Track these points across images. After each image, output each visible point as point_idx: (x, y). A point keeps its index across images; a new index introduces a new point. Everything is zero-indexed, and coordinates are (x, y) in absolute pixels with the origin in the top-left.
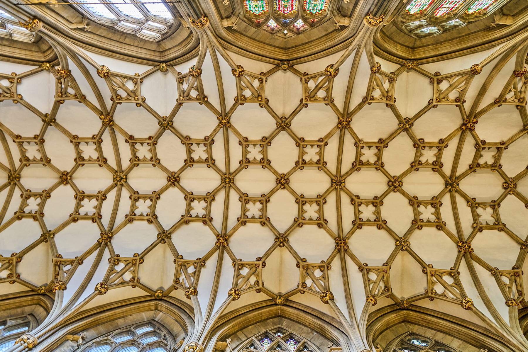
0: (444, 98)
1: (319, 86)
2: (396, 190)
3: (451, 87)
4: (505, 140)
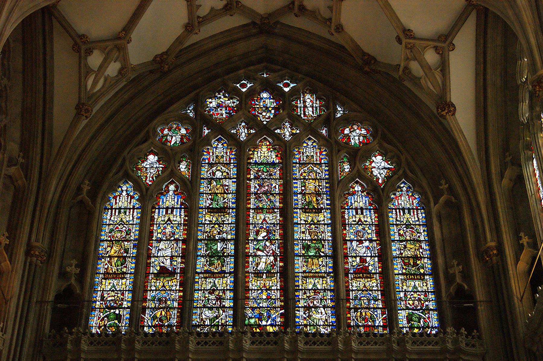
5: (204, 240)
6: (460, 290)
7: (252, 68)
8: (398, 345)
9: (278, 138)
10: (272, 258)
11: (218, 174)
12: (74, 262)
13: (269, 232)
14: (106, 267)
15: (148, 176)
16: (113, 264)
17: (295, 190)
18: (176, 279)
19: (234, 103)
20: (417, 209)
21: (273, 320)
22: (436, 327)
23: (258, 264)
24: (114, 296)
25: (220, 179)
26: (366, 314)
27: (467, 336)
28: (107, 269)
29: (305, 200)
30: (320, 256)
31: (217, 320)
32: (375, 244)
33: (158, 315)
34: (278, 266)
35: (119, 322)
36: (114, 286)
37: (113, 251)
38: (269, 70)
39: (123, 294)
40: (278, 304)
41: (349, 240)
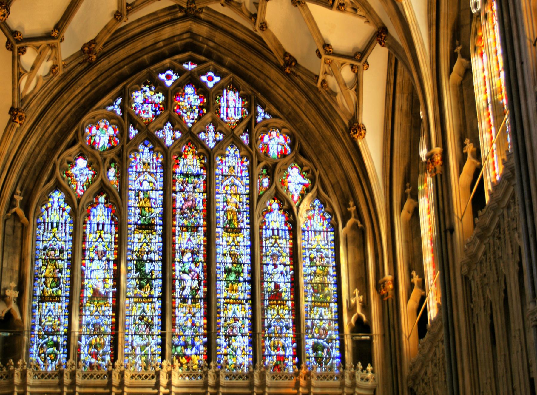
5: (134, 260)
7: (177, 57)
9: (201, 144)
10: (196, 282)
11: (146, 186)
13: (193, 253)
14: (42, 288)
15: (79, 184)
16: (49, 285)
17: (218, 205)
18: (109, 303)
20: (327, 232)
21: (197, 348)
22: (337, 358)
23: (183, 289)
24: (51, 321)
25: (147, 191)
26: (278, 343)
28: (43, 291)
29: (227, 217)
31: (147, 348)
32: (288, 268)
33: (94, 342)
34: (202, 291)
35: (58, 349)
36: (50, 310)
37: (48, 270)
38: (194, 61)
39: (59, 319)
40: (202, 331)
41: (265, 264)
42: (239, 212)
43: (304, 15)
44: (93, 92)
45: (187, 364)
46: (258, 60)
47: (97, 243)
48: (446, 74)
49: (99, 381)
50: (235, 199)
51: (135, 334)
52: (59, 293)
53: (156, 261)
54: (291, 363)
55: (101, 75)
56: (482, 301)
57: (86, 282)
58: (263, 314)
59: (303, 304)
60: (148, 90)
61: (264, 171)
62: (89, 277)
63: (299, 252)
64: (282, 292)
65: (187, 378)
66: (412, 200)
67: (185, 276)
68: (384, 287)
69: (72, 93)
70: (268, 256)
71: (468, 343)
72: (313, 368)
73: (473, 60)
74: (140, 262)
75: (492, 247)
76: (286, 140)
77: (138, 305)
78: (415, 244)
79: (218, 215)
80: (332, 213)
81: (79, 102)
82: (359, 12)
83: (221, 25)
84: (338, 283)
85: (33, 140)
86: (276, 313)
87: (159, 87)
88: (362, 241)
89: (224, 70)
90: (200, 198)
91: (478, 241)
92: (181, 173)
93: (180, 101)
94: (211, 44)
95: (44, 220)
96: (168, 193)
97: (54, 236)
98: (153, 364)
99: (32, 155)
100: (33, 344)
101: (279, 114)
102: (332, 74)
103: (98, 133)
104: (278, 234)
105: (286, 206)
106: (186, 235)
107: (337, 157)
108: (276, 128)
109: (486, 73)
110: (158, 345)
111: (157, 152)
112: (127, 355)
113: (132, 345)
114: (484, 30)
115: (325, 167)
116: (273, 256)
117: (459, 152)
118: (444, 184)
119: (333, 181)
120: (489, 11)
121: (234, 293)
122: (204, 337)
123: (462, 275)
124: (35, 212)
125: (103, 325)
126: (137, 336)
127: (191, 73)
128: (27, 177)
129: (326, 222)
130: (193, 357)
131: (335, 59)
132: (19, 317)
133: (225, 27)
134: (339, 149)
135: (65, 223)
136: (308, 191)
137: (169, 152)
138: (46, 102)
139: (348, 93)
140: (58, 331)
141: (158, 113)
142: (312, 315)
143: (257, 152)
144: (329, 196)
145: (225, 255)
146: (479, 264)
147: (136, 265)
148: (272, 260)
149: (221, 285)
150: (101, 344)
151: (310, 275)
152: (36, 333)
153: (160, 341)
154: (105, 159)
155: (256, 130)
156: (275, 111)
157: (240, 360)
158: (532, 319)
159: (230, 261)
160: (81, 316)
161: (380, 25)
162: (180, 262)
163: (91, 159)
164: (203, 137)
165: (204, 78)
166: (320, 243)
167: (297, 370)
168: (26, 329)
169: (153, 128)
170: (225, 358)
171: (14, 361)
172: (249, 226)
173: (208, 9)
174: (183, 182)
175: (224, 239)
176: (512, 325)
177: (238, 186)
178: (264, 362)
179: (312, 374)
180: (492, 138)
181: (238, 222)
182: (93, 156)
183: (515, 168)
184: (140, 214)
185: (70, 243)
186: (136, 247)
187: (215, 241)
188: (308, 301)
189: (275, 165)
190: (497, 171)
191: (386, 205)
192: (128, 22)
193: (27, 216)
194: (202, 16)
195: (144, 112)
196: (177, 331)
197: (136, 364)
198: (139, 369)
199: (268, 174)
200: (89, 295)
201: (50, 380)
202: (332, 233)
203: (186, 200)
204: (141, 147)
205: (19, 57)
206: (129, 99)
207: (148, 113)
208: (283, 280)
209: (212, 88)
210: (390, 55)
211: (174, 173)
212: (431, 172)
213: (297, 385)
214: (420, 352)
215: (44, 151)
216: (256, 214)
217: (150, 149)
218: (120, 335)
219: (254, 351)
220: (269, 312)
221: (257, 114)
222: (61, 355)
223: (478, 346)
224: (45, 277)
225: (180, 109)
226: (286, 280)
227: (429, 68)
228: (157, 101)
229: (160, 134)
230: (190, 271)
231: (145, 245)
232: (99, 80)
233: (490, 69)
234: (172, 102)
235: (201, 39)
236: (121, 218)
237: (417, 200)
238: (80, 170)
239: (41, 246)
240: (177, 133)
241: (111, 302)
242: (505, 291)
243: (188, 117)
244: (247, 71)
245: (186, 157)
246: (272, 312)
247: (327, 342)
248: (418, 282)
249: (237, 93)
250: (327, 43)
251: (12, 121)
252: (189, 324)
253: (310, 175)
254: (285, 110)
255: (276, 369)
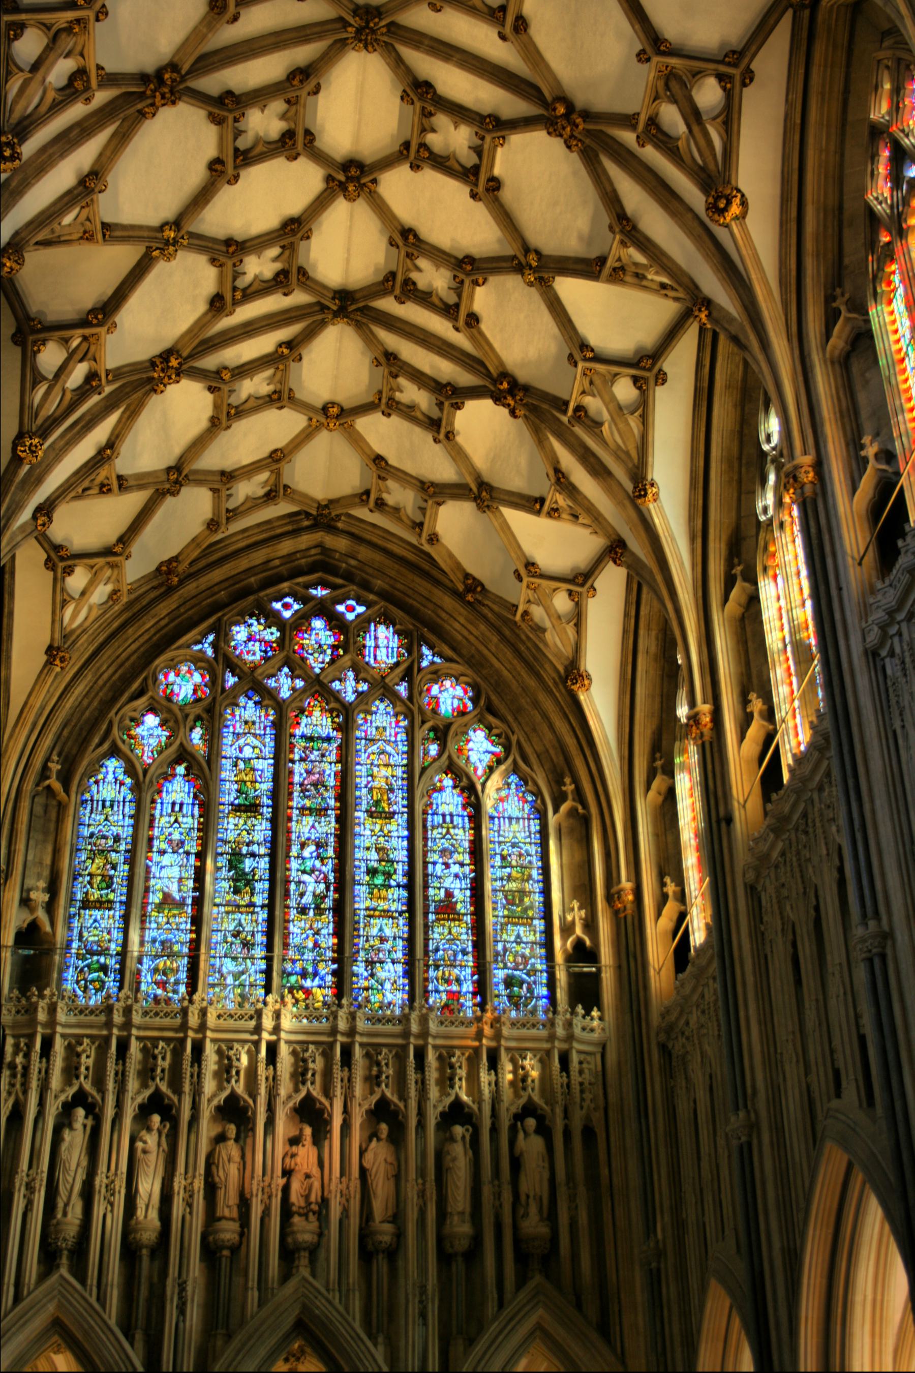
0: (591, 383)
1: (696, 129)
2: (331, 184)
3: (619, 409)
4: (459, 439)
6: (579, 944)
7: (300, 580)
8: (492, 1026)
9: (335, 696)
10: (322, 886)
11: (248, 752)
12: (42, 884)
13: (318, 845)
15: (146, 749)
16: (95, 886)
17: (358, 780)
19: (272, 634)
20: (529, 819)
21: (322, 979)
22: (543, 997)
23: (302, 895)
25: (250, 759)
27: (584, 1017)
30: (390, 886)
31: (243, 977)
32: (467, 869)
33: (161, 966)
35: (106, 975)
36: (95, 921)
37: (95, 866)
38: (325, 585)
39: (109, 933)
40: (330, 954)
42: (392, 790)
43: (496, 524)
44: (172, 625)
45: (304, 1000)
46: (424, 583)
47: (171, 830)
48: (719, 603)
49: (167, 1021)
50: (386, 772)
51: (226, 956)
52: (111, 896)
53: (260, 856)
54: (469, 1004)
55: (184, 603)
56: (779, 922)
57: (152, 882)
58: (426, 933)
59: (490, 919)
60: (255, 623)
61: (432, 735)
62: (157, 875)
63: (484, 846)
64: (456, 903)
65: (305, 1021)
66: (665, 777)
67: (305, 878)
68: (619, 898)
69: (140, 627)
70: (435, 852)
71: (756, 982)
72: (504, 1011)
73: (761, 584)
74: (236, 858)
75: (794, 844)
76: (466, 692)
77: (231, 916)
78: (670, 838)
79: (358, 793)
80: (538, 794)
81: (150, 639)
82: (581, 520)
83: (368, 536)
84: (546, 892)
85: (80, 689)
86: (446, 931)
87: (271, 619)
88: (584, 832)
89: (372, 597)
90: (330, 770)
91: (772, 836)
92: (303, 736)
93: (303, 638)
94: (353, 562)
95: (92, 797)
96: (282, 762)
97: (106, 819)
98: (252, 999)
99: (78, 708)
100: (68, 967)
101: (455, 657)
102: (539, 603)
103: (178, 680)
104: (452, 822)
105: (465, 782)
106: (310, 820)
107: (545, 717)
108: (451, 676)
109: (782, 602)
110: (261, 972)
111: (267, 707)
112: (213, 986)
113: (220, 971)
114: (778, 543)
115: (526, 729)
116: (443, 852)
117: (740, 712)
118: (716, 755)
119: (539, 748)
120: (786, 518)
121: (381, 903)
122: (333, 963)
123: (745, 884)
124: (79, 785)
125: (177, 942)
126: (229, 960)
127: (322, 600)
128: (68, 738)
129: (527, 807)
130: (314, 990)
131: (544, 583)
132: (48, 929)
133: (375, 540)
134: (549, 705)
135: (124, 802)
136: (499, 762)
137: (284, 707)
138: (101, 639)
139: (564, 629)
140: (108, 949)
141: (270, 654)
142: (505, 936)
143: (420, 708)
144: (532, 769)
145: (368, 849)
146: (773, 869)
147: (230, 861)
148: (441, 857)
149: (361, 891)
150: (172, 970)
151: (502, 879)
152: (73, 951)
153: (264, 967)
154: (186, 716)
155: (419, 678)
156: (449, 652)
157: (389, 997)
158: (861, 950)
159: (376, 857)
160: (143, 929)
161: (614, 537)
162: (298, 857)
163: (165, 715)
164: (338, 687)
165: (341, 608)
166: (518, 835)
167: (479, 1013)
168: (59, 946)
169: (261, 674)
170: (365, 994)
171: (38, 989)
172: (406, 810)
173: (349, 516)
174: (306, 748)
175: (367, 826)
176: (829, 957)
177: (390, 755)
178: (427, 1001)
179: (503, 1019)
180: (792, 692)
181: (389, 804)
182: (170, 711)
183: (831, 734)
184: (238, 791)
185: (131, 829)
186: (231, 836)
187: (353, 829)
188: (497, 916)
189: (448, 726)
190: (801, 738)
191: (623, 783)
192: (227, 533)
193: (67, 791)
194: (340, 525)
195: (248, 652)
196: (291, 953)
197: (225, 998)
198: (231, 1006)
199: (437, 738)
200: (157, 901)
201: (93, 1017)
202: (537, 822)
203: (309, 772)
204: (242, 700)
205: (63, 579)
206: (226, 635)
207: (254, 654)
208: (458, 886)
209: (353, 621)
210: (629, 579)
211: (293, 735)
212: (695, 739)
213: (479, 1035)
214: (678, 993)
215: (95, 703)
216: (418, 794)
217: (256, 703)
218: (203, 957)
219: (412, 984)
220: (436, 930)
221: (421, 656)
222: (111, 982)
223: (772, 986)
224: (90, 874)
225: (303, 649)
226: (464, 886)
227: (691, 595)
228: (268, 638)
229: (272, 683)
230: (313, 871)
231: (245, 833)
232: (182, 610)
233: (788, 596)
234: (291, 640)
235: (337, 556)
236: (209, 795)
237: (673, 777)
238: (148, 730)
239: (86, 832)
240: (297, 681)
241: (189, 910)
242: (817, 909)
243: (316, 660)
244: (407, 599)
245: (311, 714)
246: (440, 930)
247: (528, 974)
248: (674, 892)
249: (391, 629)
250: (531, 560)
251: (49, 663)
252: (310, 944)
253: (502, 740)
254: (464, 652)
255: (447, 1012)
